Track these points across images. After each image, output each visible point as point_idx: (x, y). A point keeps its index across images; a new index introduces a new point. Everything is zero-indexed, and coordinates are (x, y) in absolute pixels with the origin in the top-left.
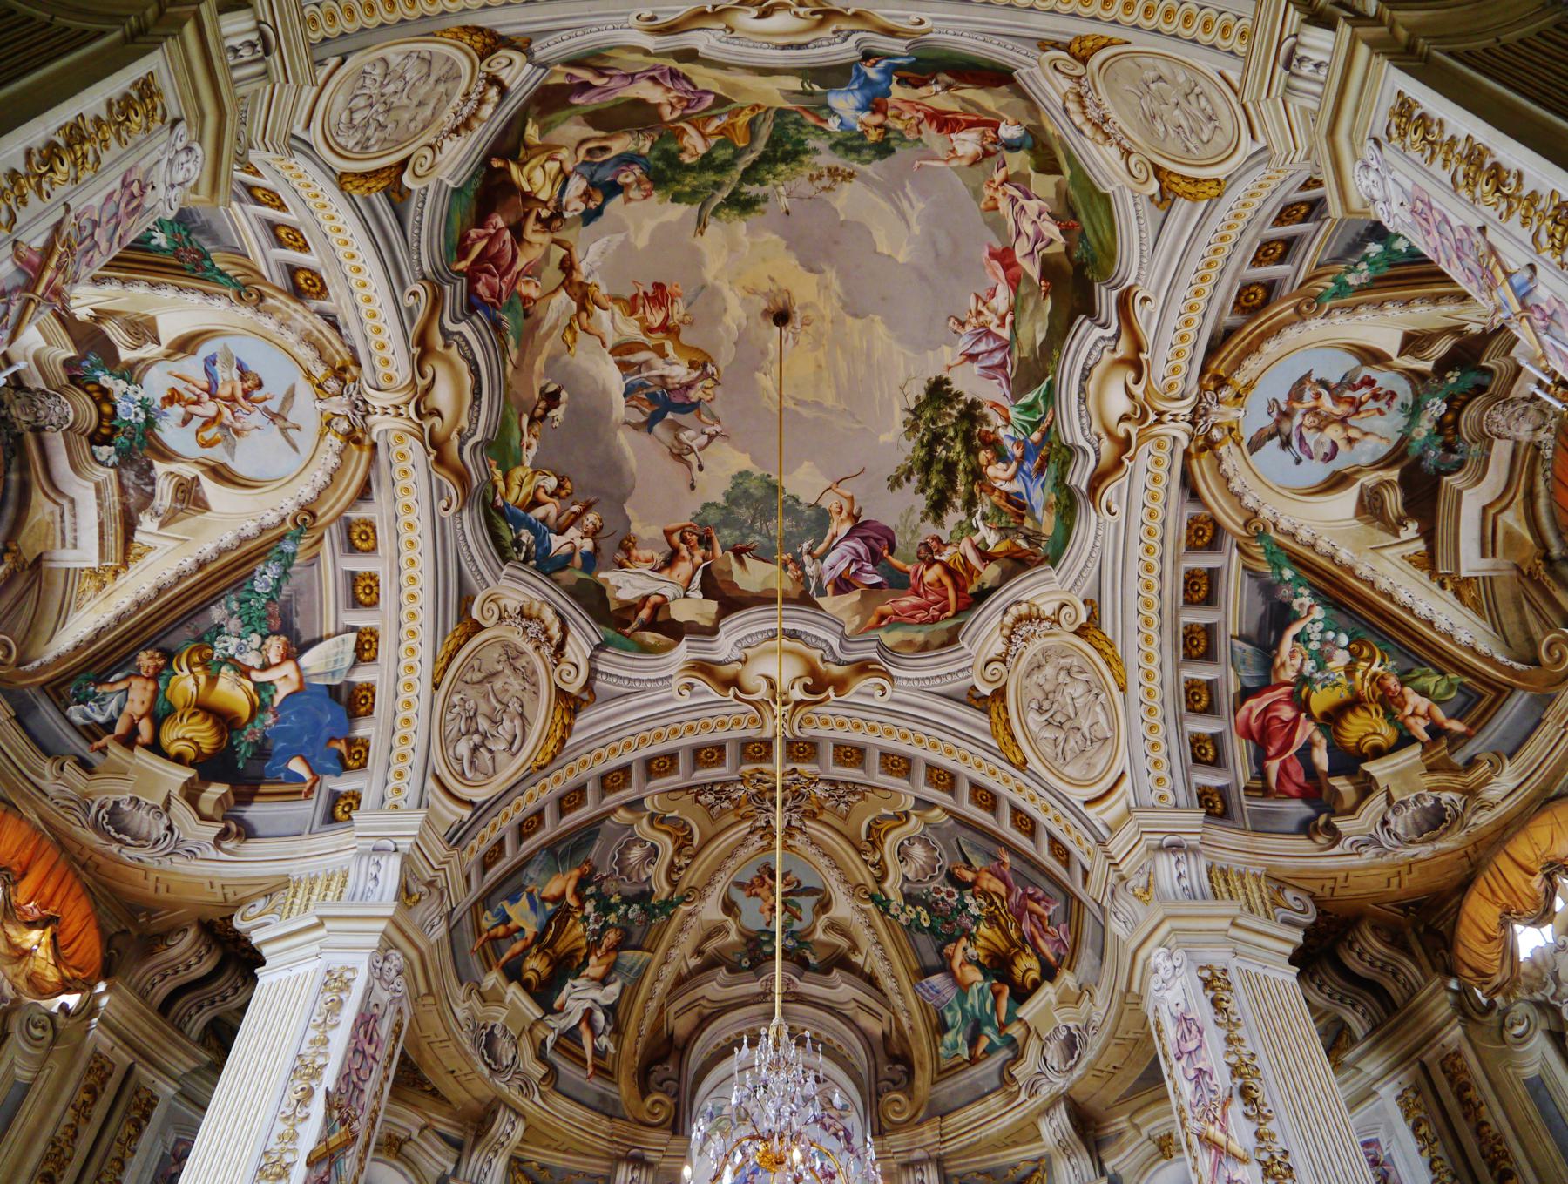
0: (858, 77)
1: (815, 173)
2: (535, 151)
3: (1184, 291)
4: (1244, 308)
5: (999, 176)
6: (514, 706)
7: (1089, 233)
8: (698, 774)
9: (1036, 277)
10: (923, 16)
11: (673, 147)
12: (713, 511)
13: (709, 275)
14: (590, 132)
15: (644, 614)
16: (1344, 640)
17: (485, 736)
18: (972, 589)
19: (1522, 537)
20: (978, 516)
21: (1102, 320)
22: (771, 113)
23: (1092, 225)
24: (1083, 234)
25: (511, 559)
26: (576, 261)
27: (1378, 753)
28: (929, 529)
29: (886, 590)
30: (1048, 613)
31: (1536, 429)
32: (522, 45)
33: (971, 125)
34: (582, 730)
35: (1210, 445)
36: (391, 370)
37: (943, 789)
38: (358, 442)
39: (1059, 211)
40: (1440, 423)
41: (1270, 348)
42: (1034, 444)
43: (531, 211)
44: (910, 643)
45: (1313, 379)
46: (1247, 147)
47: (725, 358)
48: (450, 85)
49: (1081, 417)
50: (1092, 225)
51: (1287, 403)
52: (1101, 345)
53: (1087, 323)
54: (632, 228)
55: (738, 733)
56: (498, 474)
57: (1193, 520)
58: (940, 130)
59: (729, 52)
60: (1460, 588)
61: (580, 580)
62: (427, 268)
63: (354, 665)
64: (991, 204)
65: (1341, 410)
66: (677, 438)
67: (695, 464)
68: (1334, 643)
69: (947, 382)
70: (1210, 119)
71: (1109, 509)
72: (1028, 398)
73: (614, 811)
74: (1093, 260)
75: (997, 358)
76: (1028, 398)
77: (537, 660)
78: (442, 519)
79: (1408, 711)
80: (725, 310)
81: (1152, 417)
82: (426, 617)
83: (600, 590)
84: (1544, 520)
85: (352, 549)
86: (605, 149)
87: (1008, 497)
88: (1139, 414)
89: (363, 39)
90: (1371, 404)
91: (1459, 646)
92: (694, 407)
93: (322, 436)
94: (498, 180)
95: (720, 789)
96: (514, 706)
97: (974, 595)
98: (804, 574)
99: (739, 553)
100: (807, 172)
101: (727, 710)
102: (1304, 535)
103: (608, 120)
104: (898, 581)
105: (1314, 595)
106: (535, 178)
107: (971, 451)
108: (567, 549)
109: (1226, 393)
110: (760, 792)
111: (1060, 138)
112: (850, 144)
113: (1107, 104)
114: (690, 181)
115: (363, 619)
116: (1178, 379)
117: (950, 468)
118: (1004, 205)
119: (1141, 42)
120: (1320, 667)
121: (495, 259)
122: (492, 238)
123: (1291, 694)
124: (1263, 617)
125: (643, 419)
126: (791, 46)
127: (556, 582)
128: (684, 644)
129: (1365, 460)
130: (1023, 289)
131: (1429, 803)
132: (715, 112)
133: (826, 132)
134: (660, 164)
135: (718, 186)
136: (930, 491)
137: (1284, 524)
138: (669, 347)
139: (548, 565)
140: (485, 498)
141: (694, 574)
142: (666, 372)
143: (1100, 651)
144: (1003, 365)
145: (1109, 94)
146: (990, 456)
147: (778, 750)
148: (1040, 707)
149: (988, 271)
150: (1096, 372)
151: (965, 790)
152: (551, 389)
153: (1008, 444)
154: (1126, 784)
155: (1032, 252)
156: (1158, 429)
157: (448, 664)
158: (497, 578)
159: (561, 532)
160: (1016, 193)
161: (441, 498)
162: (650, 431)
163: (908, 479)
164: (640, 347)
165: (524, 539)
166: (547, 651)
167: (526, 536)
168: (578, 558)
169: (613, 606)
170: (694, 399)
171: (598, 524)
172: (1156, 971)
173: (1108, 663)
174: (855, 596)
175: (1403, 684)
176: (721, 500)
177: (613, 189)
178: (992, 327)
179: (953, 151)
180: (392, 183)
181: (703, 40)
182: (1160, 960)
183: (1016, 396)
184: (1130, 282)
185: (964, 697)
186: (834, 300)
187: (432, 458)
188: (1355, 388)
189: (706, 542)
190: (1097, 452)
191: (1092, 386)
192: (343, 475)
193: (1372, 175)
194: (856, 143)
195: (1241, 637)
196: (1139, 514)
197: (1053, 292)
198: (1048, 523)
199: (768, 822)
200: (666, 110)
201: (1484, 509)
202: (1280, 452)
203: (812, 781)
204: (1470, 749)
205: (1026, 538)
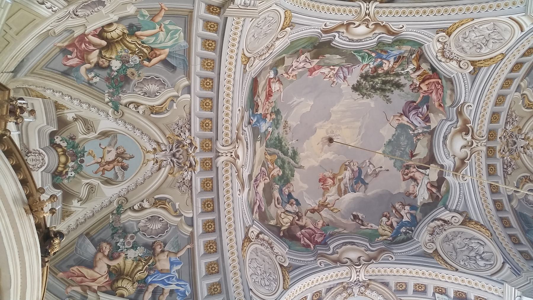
0: (256, 125)
1: (285, 133)
2: (278, 221)
3: (323, 14)
5: (286, 75)
6: (467, 241)
7: (303, 46)
8: (499, 174)
9: (318, 60)
10: (237, 110)
11: (277, 178)
12: (396, 164)
13: (317, 164)
14: (273, 204)
15: (434, 190)
17: (477, 254)
18: (430, 73)
20: (403, 72)
21: (333, 38)
22: (267, 149)
23: (301, 45)
25: (411, 236)
26: (311, 208)
28: (407, 89)
29: (429, 104)
30: (441, 46)
32: (248, 228)
33: (270, 87)
34: (477, 217)
36: (345, 273)
37: (512, 82)
38: (368, 285)
39: (296, 56)
42: (376, 55)
43: (296, 223)
44: (451, 96)
46: (274, 7)
47: (344, 159)
48: (259, 251)
49: (367, 41)
50: (301, 45)
53: (334, 42)
54: (302, 189)
55: (483, 160)
56: (380, 238)
58: (272, 96)
59: (249, 165)
61: (420, 212)
62: (312, 259)
63: (447, 296)
64: (294, 77)
66: (370, 175)
67: (380, 169)
69: (353, 86)
72: (360, 58)
73: (512, 207)
74: (312, 43)
75: (345, 70)
76: (360, 58)
77: (450, 230)
78: (396, 260)
80: (328, 159)
81: (367, 17)
82: (431, 270)
83: (424, 205)
85: (405, 291)
86: (278, 199)
87: (395, 62)
88: (366, 22)
89: (245, 283)
92: (360, 169)
93: (366, 296)
94: (286, 234)
95: (506, 166)
96: (467, 241)
97: (433, 72)
98: (422, 133)
99: (412, 156)
100: (285, 135)
101: (474, 164)
103: (269, 200)
104: (426, 100)
106: (286, 221)
107: (378, 76)
108: (408, 215)
110: (509, 151)
111: (273, 59)
112: (276, 123)
114: (288, 172)
115: (430, 291)
117: (384, 83)
118: (295, 73)
119: (243, 45)
121: (311, 235)
122: (304, 236)
125: (363, 186)
126: (247, 147)
127: (420, 220)
128: (446, 177)
130: (322, 64)
132: (267, 166)
133: (273, 131)
134: (282, 181)
135: (289, 163)
136: (393, 89)
138: (340, 177)
139: (414, 223)
140: (389, 244)
141: (420, 172)
142: (348, 178)
143: (457, 28)
144: (348, 68)
146: (380, 69)
147: (491, 144)
148: (479, 48)
149: (316, 76)
150: (350, 37)
151: (513, 74)
152: (352, 217)
153: (376, 64)
154: (515, 17)
156: (372, 14)
157: (449, 264)
158: (418, 242)
159: (402, 217)
160: (291, 70)
161: (388, 260)
162: (368, 184)
163: (388, 97)
164: (339, 187)
165: (404, 231)
166: (446, 227)
167: (403, 230)
168: (412, 212)
169: (431, 201)
170: (357, 169)
171: (400, 203)
173: (462, 25)
174: (431, 115)
176: (393, 161)
177: (290, 196)
178: (334, 73)
179: (278, 91)
180: (287, 270)
181: (246, 174)
183: (358, 62)
184: (319, 31)
185: (474, 76)
186: (325, 123)
187: (374, 261)
189: (408, 167)
190: (380, 34)
191: (355, 38)
192: (380, 291)
194: (276, 121)
197: (323, 55)
198: (406, 48)
199: (522, 147)
200: (266, 181)
203: (505, 130)
205: (411, 55)
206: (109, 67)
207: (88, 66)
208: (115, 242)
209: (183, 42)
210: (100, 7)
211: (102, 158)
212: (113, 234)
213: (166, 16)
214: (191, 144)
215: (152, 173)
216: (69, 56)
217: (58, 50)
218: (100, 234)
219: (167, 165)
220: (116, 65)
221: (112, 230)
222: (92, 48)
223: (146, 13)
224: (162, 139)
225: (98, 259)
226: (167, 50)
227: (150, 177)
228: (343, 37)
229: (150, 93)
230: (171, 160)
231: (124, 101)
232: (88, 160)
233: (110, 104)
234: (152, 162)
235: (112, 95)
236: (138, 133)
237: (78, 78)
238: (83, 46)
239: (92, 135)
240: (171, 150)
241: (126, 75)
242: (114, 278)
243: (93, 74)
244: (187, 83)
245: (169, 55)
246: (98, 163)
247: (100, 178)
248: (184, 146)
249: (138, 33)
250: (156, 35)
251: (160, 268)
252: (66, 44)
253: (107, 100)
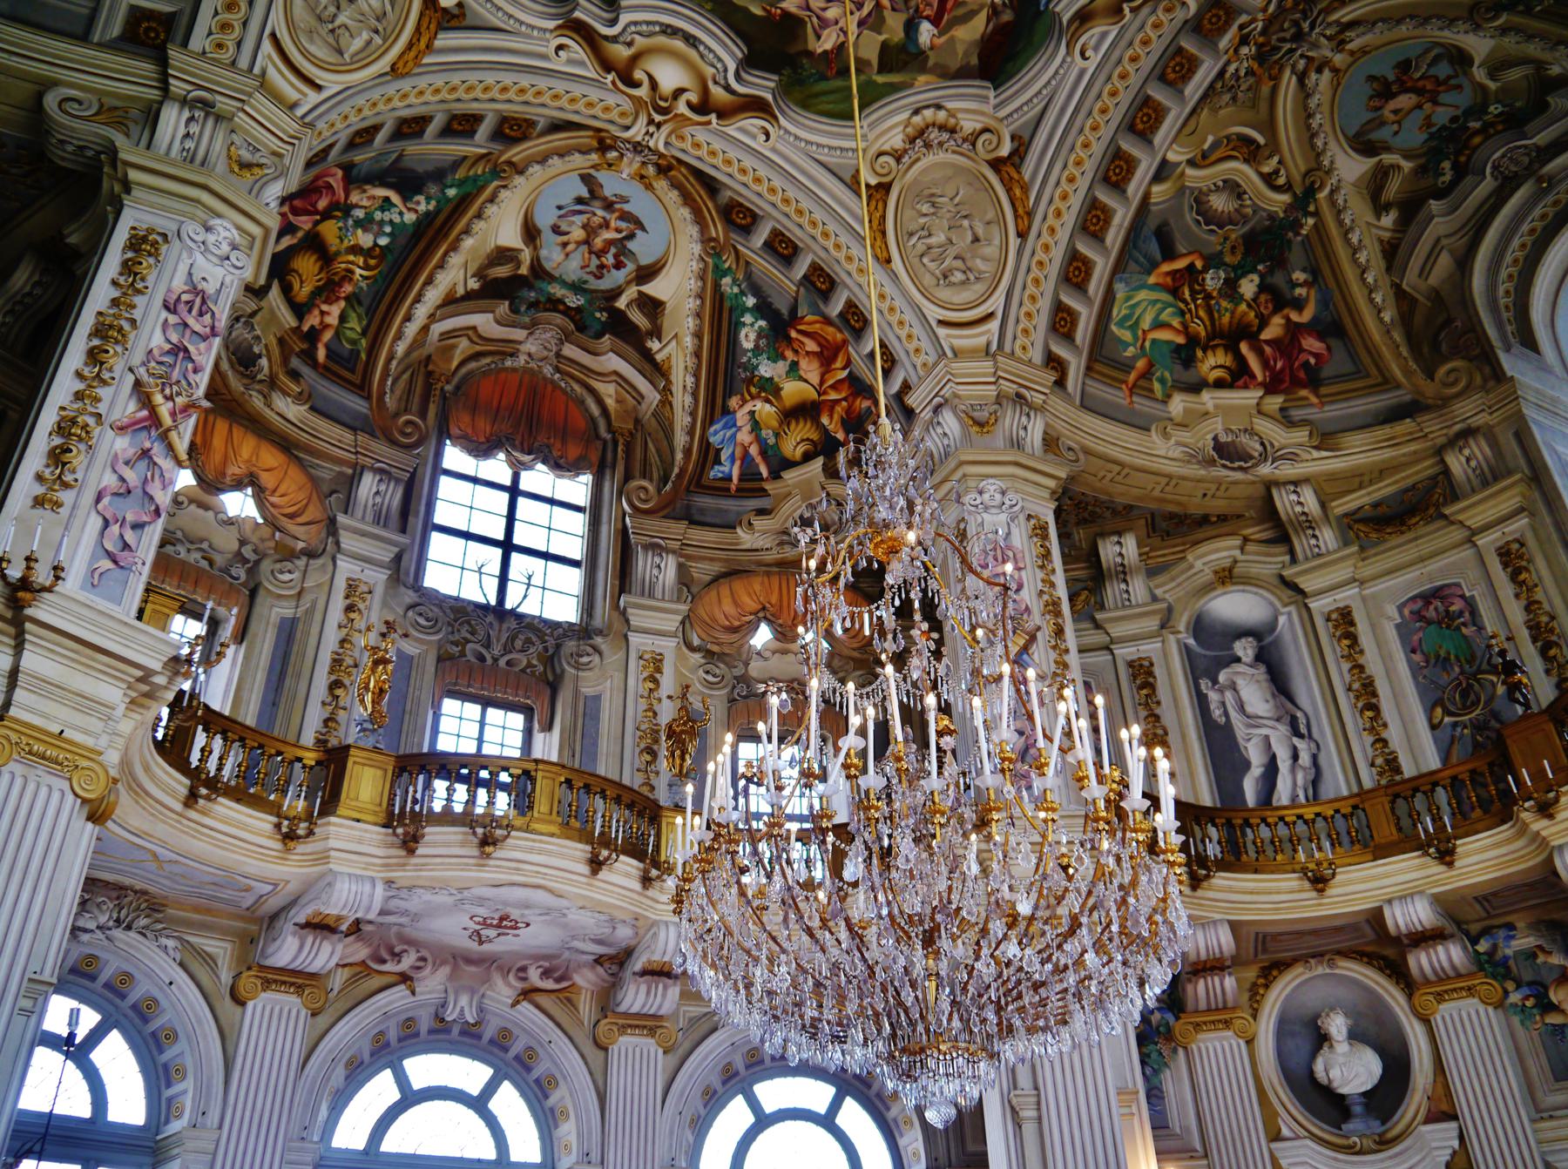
4: (733, 207)
7: (823, 86)
9: (783, 5)
16: (383, 241)
19: (450, 359)
21: (744, 75)
24: (824, 78)
27: (287, 290)
31: (530, 355)
35: (603, 148)
40: (561, 301)
41: (685, 212)
45: (639, 233)
49: (648, 23)
51: (621, 210)
52: (719, 66)
53: (740, 55)
57: (531, 124)
60: (425, 329)
65: (598, 242)
68: (380, 233)
70: (945, 277)
71: (560, 47)
74: (801, 82)
79: (325, 307)
84: (464, 370)
88: (660, 106)
90: (595, 262)
91: (392, 346)
102: (491, 210)
105: (428, 213)
109: (651, 170)
111: (911, 85)
113: (942, 156)
116: (687, 145)
120: (359, 223)
123: (338, 203)
124: (412, 171)
129: (544, 253)
131: (256, 350)
137: (503, 194)
143: (418, 30)
145: (954, 165)
154: (313, 97)
155: (808, 8)
156: (643, 120)
160: (865, 11)
172: (208, 229)
173: (410, 46)
175: (347, 299)
182: (224, 233)
188: (616, 256)
191: (679, 44)
193: (998, 497)
195: (401, 156)
196: (560, 86)
201: (474, 328)
202: (575, 194)
204: (305, 370)
206: (1262, 288)
207: (1295, 317)
209: (1120, 290)
210: (1223, 438)
211: (1419, 106)
213: (1127, 367)
214: (1244, 40)
215: (1374, 24)
216: (1312, 361)
217: (1323, 390)
219: (1329, 24)
220: (1248, 287)
222: (1268, 350)
223: (1157, 386)
224: (1288, 82)
226: (1152, 280)
227: (1383, 20)
228: (715, 61)
229: (1232, 191)
230: (1312, 27)
231: (1285, 198)
232: (1442, 116)
233: (1312, 208)
234: (1349, 47)
235: (1296, 226)
236: (1315, 123)
237: (1325, 302)
238: (1279, 365)
239: (1388, 158)
240: (1292, 51)
241: (1246, 254)
243: (1298, 291)
244: (1156, 189)
245: (1154, 265)
246: (1436, 103)
247: (1467, 74)
248: (1262, 45)
249: (1181, 340)
250: (1159, 325)
252: (1304, 393)
253: (1311, 221)
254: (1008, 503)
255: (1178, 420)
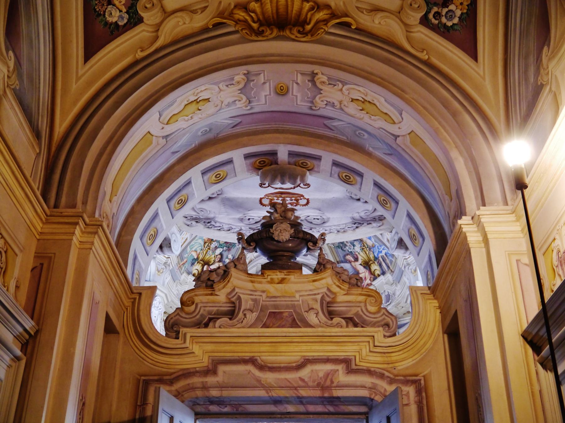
193: (158, 303)
206: (221, 254)
208: (347, 251)
212: (342, 249)
218: (340, 256)
220: (218, 251)
221: (339, 248)
225: (355, 267)
242: (368, 268)
250: (196, 251)
251: (371, 245)
254: (159, 307)
255: (181, 282)
